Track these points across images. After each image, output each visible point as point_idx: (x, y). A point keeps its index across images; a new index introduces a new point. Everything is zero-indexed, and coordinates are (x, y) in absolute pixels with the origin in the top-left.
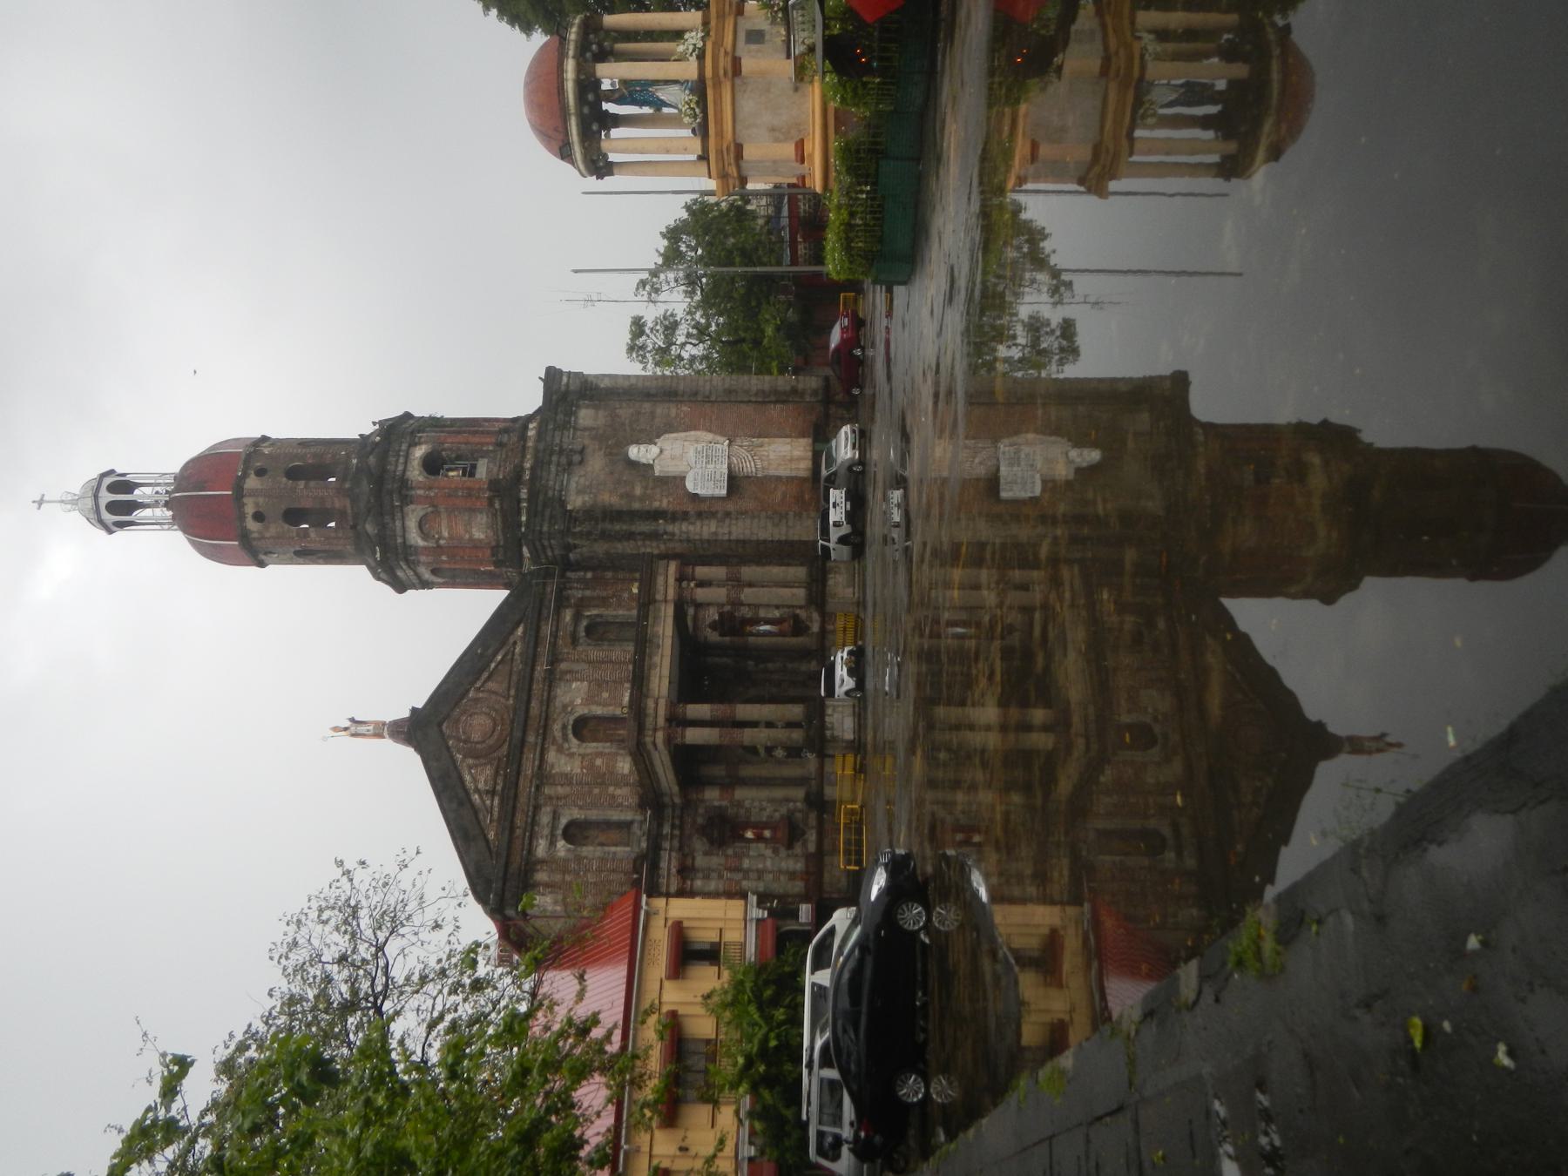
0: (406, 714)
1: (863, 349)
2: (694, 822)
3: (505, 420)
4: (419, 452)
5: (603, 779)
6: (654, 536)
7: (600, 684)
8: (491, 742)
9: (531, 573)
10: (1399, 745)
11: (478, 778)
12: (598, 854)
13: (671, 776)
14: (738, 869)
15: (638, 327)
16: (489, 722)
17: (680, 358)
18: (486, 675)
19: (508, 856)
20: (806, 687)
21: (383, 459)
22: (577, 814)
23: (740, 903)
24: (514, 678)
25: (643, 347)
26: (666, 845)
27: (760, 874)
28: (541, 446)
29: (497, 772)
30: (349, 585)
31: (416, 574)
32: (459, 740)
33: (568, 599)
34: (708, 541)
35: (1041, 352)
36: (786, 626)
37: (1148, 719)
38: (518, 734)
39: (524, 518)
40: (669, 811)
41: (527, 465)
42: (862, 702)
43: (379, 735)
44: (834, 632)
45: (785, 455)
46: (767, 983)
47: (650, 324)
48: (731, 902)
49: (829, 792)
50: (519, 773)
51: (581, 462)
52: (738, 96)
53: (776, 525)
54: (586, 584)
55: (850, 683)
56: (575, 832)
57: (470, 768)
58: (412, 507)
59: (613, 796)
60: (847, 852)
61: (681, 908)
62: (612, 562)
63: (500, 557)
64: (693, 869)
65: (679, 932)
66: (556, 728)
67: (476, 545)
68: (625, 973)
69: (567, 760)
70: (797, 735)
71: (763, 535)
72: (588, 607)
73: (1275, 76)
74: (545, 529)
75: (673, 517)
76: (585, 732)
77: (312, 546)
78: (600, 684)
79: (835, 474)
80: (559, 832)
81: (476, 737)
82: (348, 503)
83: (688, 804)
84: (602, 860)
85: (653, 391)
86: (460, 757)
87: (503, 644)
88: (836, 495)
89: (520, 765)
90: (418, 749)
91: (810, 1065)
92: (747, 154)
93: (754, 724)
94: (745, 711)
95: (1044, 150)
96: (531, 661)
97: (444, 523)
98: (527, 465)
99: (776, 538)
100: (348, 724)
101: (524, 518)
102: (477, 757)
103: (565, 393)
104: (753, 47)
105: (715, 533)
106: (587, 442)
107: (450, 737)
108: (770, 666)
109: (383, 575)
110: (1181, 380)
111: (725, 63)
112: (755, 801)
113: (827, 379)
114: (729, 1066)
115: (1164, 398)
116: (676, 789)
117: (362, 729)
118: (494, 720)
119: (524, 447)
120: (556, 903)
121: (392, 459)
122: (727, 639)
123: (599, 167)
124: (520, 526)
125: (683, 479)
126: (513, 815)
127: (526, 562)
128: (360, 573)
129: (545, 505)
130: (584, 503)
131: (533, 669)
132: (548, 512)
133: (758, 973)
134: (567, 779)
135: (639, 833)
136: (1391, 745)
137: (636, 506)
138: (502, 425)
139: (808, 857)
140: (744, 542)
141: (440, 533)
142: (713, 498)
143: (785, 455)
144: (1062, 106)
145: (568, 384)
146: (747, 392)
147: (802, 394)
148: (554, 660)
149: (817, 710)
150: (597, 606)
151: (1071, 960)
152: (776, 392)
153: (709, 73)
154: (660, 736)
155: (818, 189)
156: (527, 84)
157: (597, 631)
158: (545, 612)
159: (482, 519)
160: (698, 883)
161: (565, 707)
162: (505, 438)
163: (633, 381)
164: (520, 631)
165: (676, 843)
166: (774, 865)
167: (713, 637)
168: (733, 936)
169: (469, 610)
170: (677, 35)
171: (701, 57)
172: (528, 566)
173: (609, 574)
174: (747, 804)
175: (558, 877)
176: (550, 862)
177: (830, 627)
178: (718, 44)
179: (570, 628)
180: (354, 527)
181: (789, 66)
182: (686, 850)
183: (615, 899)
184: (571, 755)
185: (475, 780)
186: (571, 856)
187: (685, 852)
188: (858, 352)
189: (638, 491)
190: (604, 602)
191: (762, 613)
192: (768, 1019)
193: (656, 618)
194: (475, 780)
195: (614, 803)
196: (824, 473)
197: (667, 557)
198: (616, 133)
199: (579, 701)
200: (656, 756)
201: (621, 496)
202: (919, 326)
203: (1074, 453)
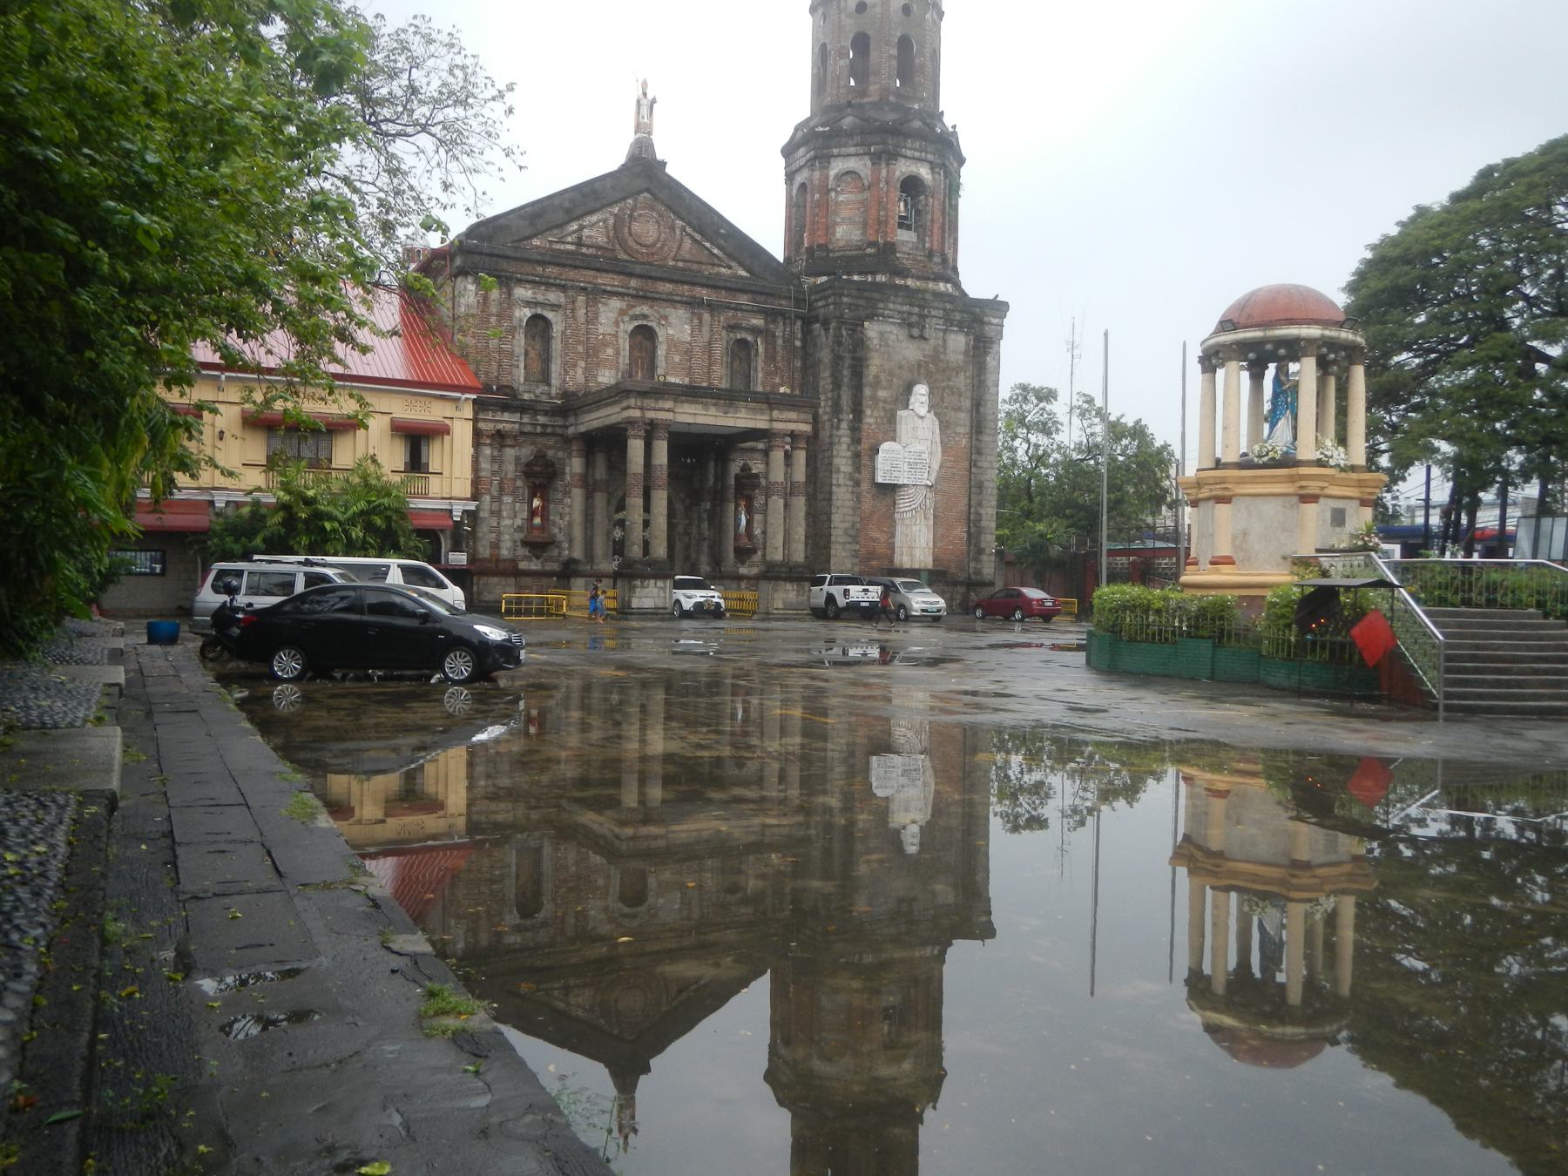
0: (659, 157)
1: (1021, 620)
2: (550, 448)
3: (955, 260)
4: (924, 172)
5: (592, 354)
6: (836, 408)
7: (688, 353)
8: (631, 243)
9: (801, 284)
12: (517, 350)
13: (596, 424)
14: (501, 489)
15: (1047, 395)
18: (698, 237)
19: (516, 259)
20: (682, 563)
22: (557, 328)
24: (695, 267)
26: (526, 419)
27: (497, 514)
28: (928, 296)
29: (598, 248)
31: (801, 168)
32: (633, 209)
33: (774, 321)
36: (745, 540)
37: (651, 900)
38: (638, 269)
39: (856, 278)
40: (559, 421)
41: (910, 282)
43: (638, 128)
44: (739, 589)
45: (916, 541)
46: (388, 519)
47: (1048, 407)
49: (578, 585)
51: (911, 337)
52: (1280, 500)
54: (788, 341)
55: (688, 605)
57: (605, 221)
58: (869, 164)
59: (575, 366)
60: (519, 601)
61: (462, 433)
62: (809, 368)
64: (503, 446)
65: (439, 431)
67: (829, 229)
68: (397, 377)
69: (611, 320)
70: (636, 551)
71: (836, 518)
72: (766, 342)
73: (1289, 1030)
74: (845, 299)
77: (831, 61)
78: (688, 353)
79: (897, 591)
80: (539, 311)
81: (636, 227)
82: (874, 98)
83: (567, 441)
84: (512, 354)
86: (616, 210)
87: (730, 256)
88: (875, 593)
89: (606, 271)
90: (623, 168)
91: (307, 563)
93: (647, 509)
94: (660, 499)
95: (1218, 805)
96: (713, 284)
97: (852, 197)
98: (910, 282)
99: (833, 532)
100: (650, 97)
101: (856, 278)
102: (615, 227)
103: (980, 323)
104: (1328, 516)
105: (838, 471)
106: (932, 342)
108: (705, 525)
109: (800, 134)
110: (987, 932)
111: (1313, 487)
112: (570, 508)
113: (991, 584)
114: (308, 483)
115: (970, 916)
116: (582, 429)
117: (645, 111)
118: (653, 245)
119: (927, 279)
121: (917, 145)
122: (732, 482)
123: (1212, 359)
125: (894, 439)
127: (812, 280)
129: (868, 299)
131: (703, 286)
133: (397, 511)
134: (592, 319)
135: (538, 391)
136: (626, 1138)
137: (867, 392)
138: (950, 256)
139: (514, 561)
141: (842, 192)
143: (916, 541)
144: (1264, 822)
146: (980, 504)
147: (977, 560)
148: (712, 307)
149: (661, 571)
150: (766, 350)
152: (980, 532)
154: (637, 413)
155: (1183, 579)
156: (1296, 287)
157: (741, 351)
158: (762, 298)
159: (855, 235)
160: (487, 451)
161: (666, 318)
162: (937, 260)
163: (992, 390)
164: (743, 273)
165: (528, 429)
166: (506, 527)
167: (735, 468)
168: (435, 485)
169: (764, 221)
170: (1342, 440)
171: (1320, 463)
172: (808, 281)
173: (798, 364)
175: (494, 309)
177: (743, 584)
178: (1331, 480)
179: (744, 323)
180: (849, 104)
181: (1307, 551)
182: (521, 439)
183: (472, 367)
184: (617, 324)
185: (592, 225)
186: (515, 322)
187: (521, 436)
188: (1018, 615)
189: (882, 394)
190: (771, 357)
191: (758, 517)
192: (352, 521)
193: (754, 410)
195: (568, 366)
196: (898, 581)
197: (816, 421)
198: (1245, 375)
199: (671, 332)
200: (616, 409)
201: (876, 377)
202: (1044, 676)
203: (915, 829)
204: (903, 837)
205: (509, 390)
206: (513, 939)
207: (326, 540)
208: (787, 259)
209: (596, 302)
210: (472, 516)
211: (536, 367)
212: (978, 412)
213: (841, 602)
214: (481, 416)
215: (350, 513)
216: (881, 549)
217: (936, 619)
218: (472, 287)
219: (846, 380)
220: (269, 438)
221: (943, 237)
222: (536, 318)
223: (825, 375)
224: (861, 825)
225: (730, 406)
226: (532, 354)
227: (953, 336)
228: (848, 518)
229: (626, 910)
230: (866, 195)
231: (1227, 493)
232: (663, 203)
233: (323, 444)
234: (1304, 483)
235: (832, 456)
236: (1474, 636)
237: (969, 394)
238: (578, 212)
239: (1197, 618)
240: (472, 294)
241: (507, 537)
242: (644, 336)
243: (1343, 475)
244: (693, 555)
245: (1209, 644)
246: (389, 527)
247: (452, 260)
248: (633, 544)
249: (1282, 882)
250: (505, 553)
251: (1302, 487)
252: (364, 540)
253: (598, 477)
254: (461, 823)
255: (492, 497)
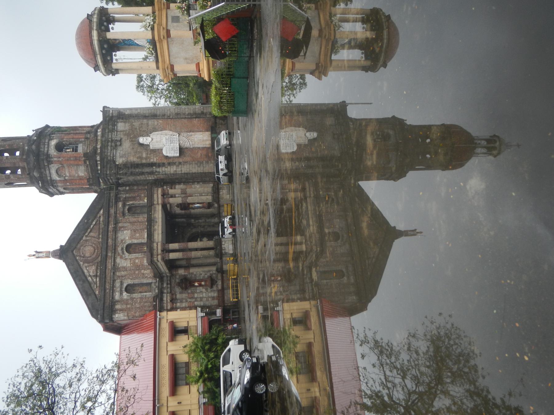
0: (58, 248)
2: (175, 281)
3: (88, 127)
4: (53, 143)
5: (138, 268)
6: (152, 173)
7: (135, 231)
8: (94, 256)
9: (104, 188)
10: (421, 233)
11: (90, 271)
12: (139, 296)
13: (165, 268)
14: (192, 298)
16: (92, 248)
17: (158, 89)
18: (89, 230)
19: (104, 300)
22: (130, 282)
23: (195, 311)
25: (142, 86)
26: (165, 291)
27: (201, 299)
28: (104, 139)
32: (80, 256)
33: (120, 198)
34: (173, 174)
35: (294, 84)
38: (104, 253)
39: (99, 168)
40: (165, 279)
41: (99, 147)
42: (234, 236)
43: (48, 257)
44: (223, 206)
46: (206, 344)
47: (145, 77)
48: (191, 311)
49: (225, 267)
50: (106, 268)
51: (121, 145)
52: (170, 46)
53: (199, 167)
54: (127, 192)
55: (230, 230)
56: (129, 289)
57: (86, 267)
58: (52, 165)
59: (143, 274)
60: (233, 287)
61: (173, 316)
62: (136, 183)
63: (91, 182)
64: (176, 299)
65: (173, 325)
66: (119, 249)
67: (81, 178)
68: (153, 336)
69: (125, 261)
70: (212, 253)
72: (128, 201)
74: (108, 172)
75: (159, 165)
76: (131, 250)
77: (12, 181)
78: (135, 231)
79: (220, 149)
80: (124, 289)
81: (87, 255)
83: (172, 275)
84: (141, 298)
85: (147, 115)
86: (81, 263)
87: (95, 217)
88: (221, 158)
89: (106, 265)
92: (176, 69)
94: (192, 245)
96: (107, 224)
98: (99, 147)
99: (199, 171)
100: (34, 253)
102: (88, 263)
103: (112, 118)
104: (175, 24)
105: (176, 171)
106: (122, 136)
107: (77, 256)
108: (200, 221)
109: (43, 191)
110: (344, 105)
111: (163, 33)
114: (195, 369)
116: (167, 271)
117: (40, 255)
118: (94, 248)
119: (97, 140)
120: (124, 316)
121: (42, 146)
122: (183, 211)
123: (111, 71)
124: (98, 171)
125: (162, 150)
126: (105, 284)
127: (102, 184)
128: (33, 191)
129: (107, 162)
130: (123, 161)
132: (108, 166)
133: (203, 340)
134: (125, 269)
135: (154, 287)
136: (418, 233)
137: (144, 161)
139: (218, 291)
140: (187, 174)
142: (174, 157)
143: (200, 139)
145: (112, 113)
146: (184, 114)
147: (206, 114)
148: (116, 223)
149: (219, 243)
151: (314, 319)
152: (195, 114)
153: (156, 38)
154: (159, 257)
155: (206, 78)
156: (77, 39)
157: (132, 210)
158: (111, 204)
160: (178, 304)
161: (122, 241)
162: (89, 136)
163: (139, 111)
164: (102, 212)
165: (169, 290)
167: (178, 211)
168: (192, 323)
169: (81, 203)
171: (153, 29)
174: (195, 273)
175: (124, 306)
176: (121, 301)
178: (160, 25)
179: (121, 210)
182: (173, 292)
183: (147, 312)
184: (126, 259)
185: (89, 272)
186: (129, 298)
189: (144, 155)
190: (134, 198)
192: (207, 356)
193: (155, 211)
194: (89, 272)
196: (216, 149)
200: (159, 264)
201: (138, 158)
203: (308, 134)
204: (312, 138)
205: (155, 298)
206: (352, 280)
207: (215, 366)
208: (95, 192)
209: (118, 268)
210: (203, 308)
211: (145, 288)
212: (148, 117)
213: (225, 171)
214: (165, 308)
215: (205, 358)
216: (204, 152)
217: (230, 133)
218: (117, 315)
219: (140, 170)
220: (179, 385)
221: (79, 133)
222: (127, 290)
223: (139, 178)
224: (307, 155)
225: (153, 220)
226: (141, 290)
227: (119, 128)
228: (193, 166)
229: (340, 240)
230: (65, 165)
231: (169, 67)
232: (77, 245)
233: (180, 365)
234: (162, 37)
235: (170, 174)
237: (141, 120)
238: (84, 278)
239: (223, 84)
240: (119, 315)
241: (210, 294)
242: (130, 248)
243: (157, 18)
244: (212, 224)
245: (232, 79)
246: (209, 343)
247: (107, 323)
248: (209, 254)
249: (328, 41)
250: (216, 295)
251: (164, 38)
252: (215, 352)
253: (185, 263)
254: (313, 302)
255: (195, 301)
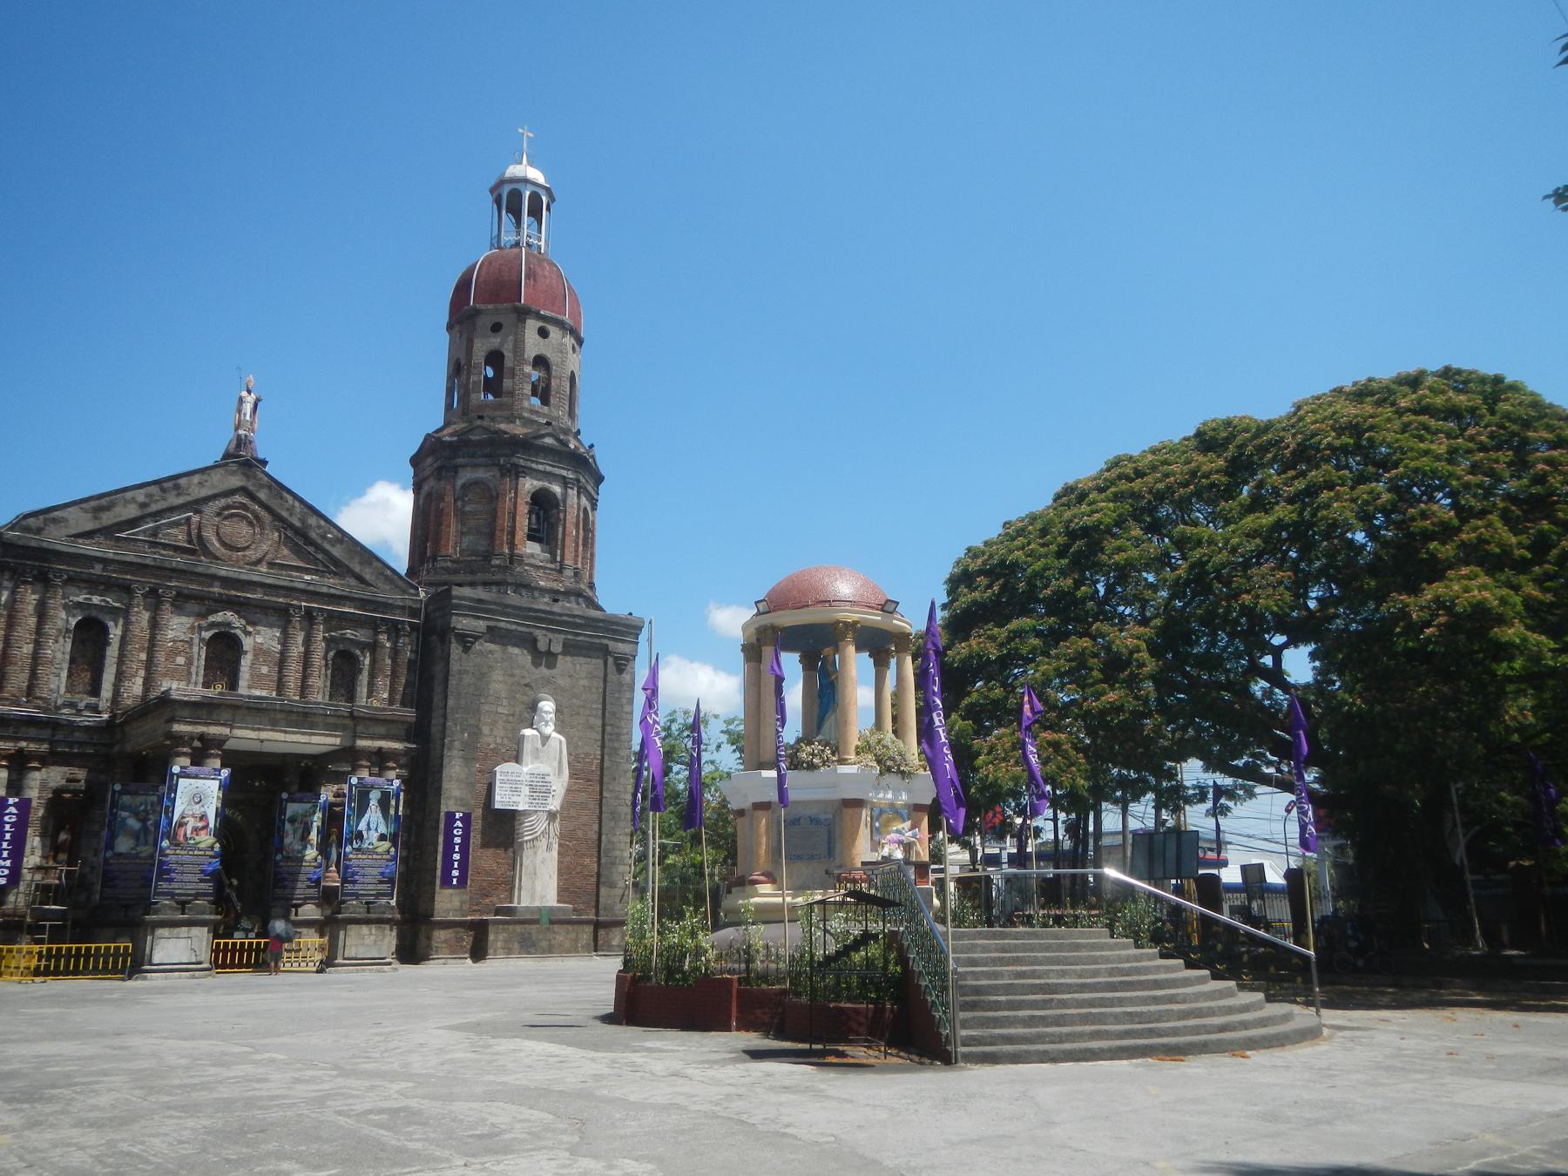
3: (591, 576)
21: (547, 451)
29: (176, 549)
30: (425, 410)
38: (224, 571)
57: (188, 519)
58: (498, 475)
66: (229, 616)
80: (94, 613)
163: (627, 709)
199: (259, 640)
236: (1017, 961)
238: (154, 508)
